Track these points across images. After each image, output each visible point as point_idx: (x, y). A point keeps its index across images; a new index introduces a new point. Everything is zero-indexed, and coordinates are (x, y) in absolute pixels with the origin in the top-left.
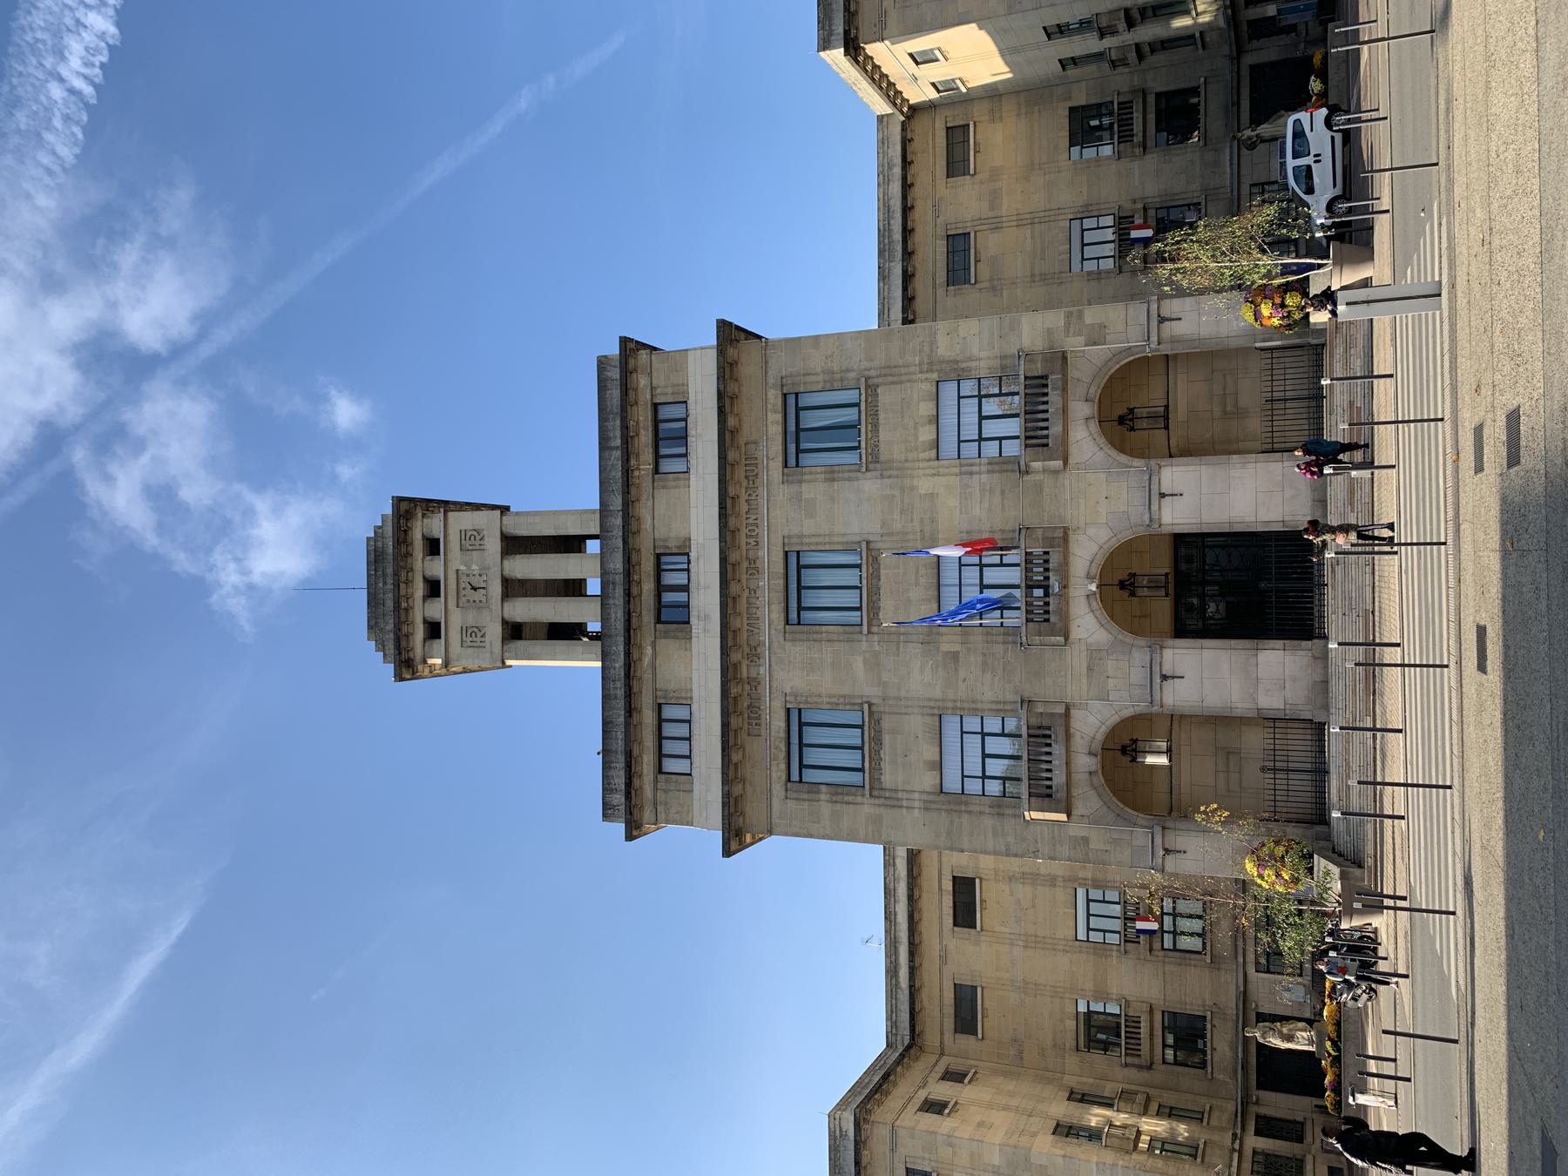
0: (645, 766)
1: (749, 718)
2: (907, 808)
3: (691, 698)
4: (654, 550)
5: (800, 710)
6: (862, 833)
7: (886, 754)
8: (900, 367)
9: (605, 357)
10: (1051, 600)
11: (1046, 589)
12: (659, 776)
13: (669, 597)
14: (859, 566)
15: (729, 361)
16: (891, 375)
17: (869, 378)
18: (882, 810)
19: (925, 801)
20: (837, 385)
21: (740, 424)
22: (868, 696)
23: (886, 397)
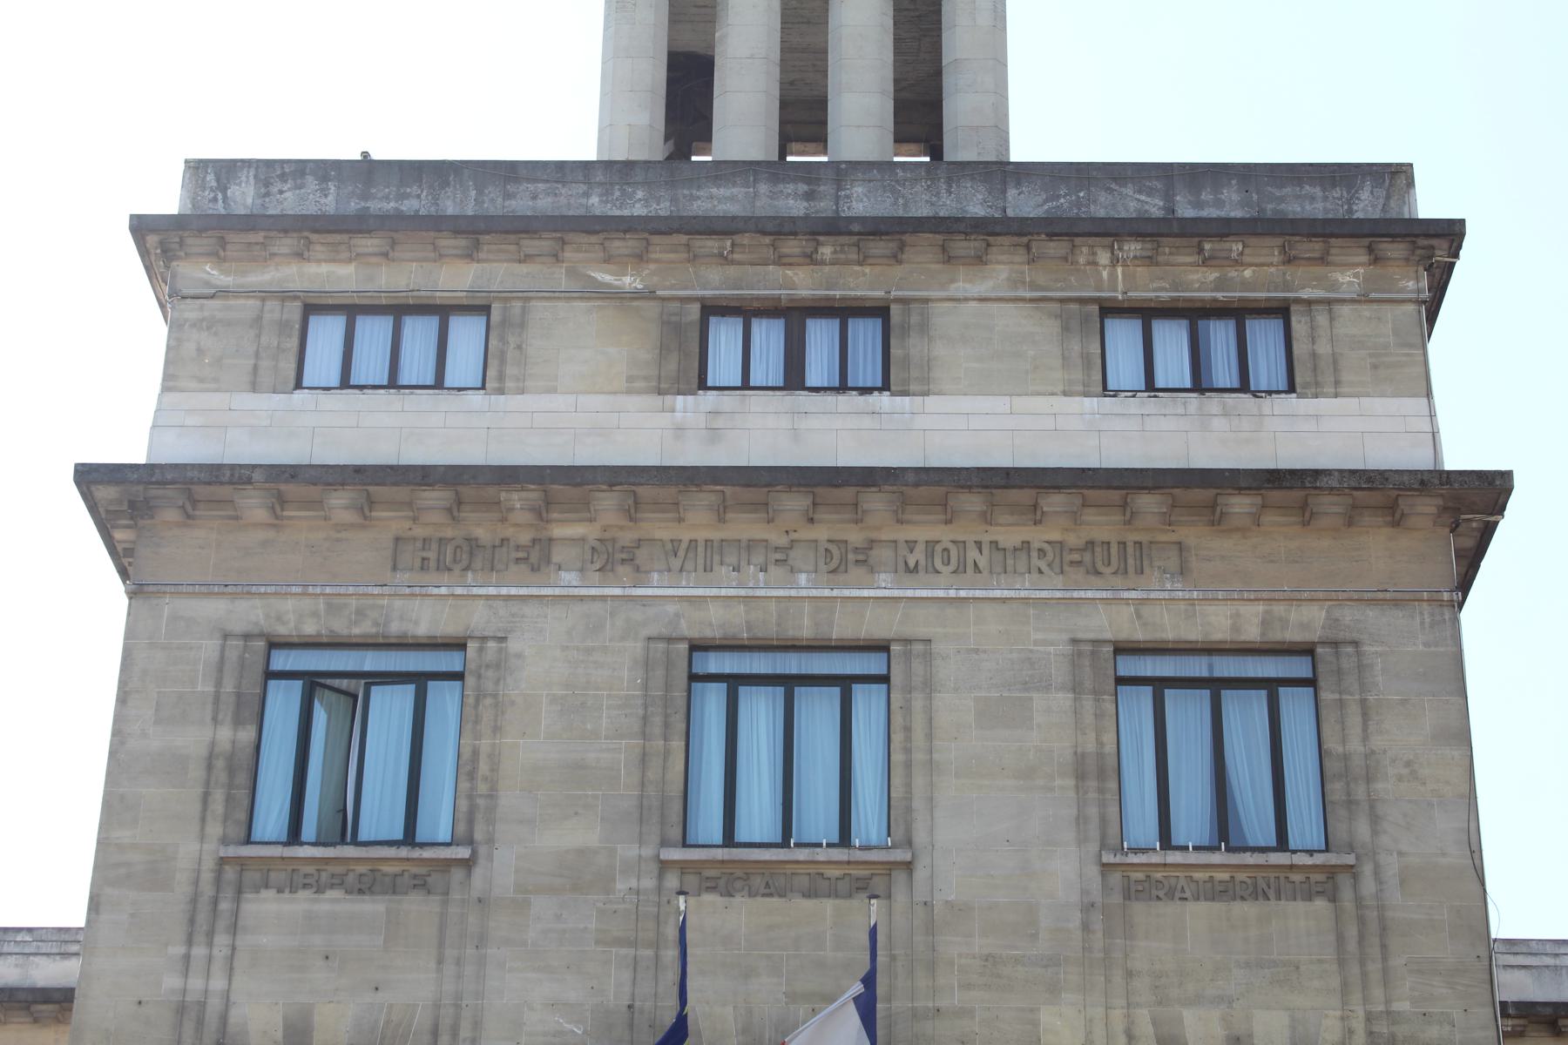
0: (324, 268)
2: (187, 958)
3: (501, 391)
5: (458, 676)
6: (123, 835)
7: (333, 903)
8: (1385, 959)
9: (1411, 183)
12: (298, 304)
13: (769, 337)
14: (845, 839)
15: (1403, 504)
18: (182, 888)
19: (202, 1005)
20: (1336, 789)
21: (1237, 529)
22: (490, 858)
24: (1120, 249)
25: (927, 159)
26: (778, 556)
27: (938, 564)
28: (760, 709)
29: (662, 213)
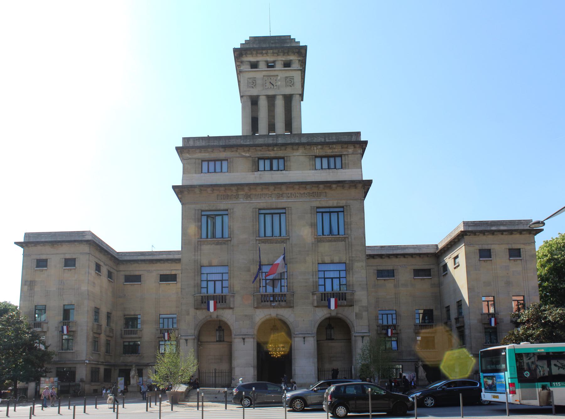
0: (204, 154)
1: (224, 195)
2: (195, 254)
3: (230, 172)
4: (286, 156)
5: (227, 215)
10: (269, 303)
11: (273, 301)
12: (201, 160)
13: (268, 162)
14: (280, 235)
16: (348, 247)
17: (348, 238)
19: (197, 260)
20: (346, 226)
23: (341, 245)
24: (318, 147)
25: (290, 133)
26: (270, 196)
27: (292, 196)
28: (268, 218)
29: (252, 144)
